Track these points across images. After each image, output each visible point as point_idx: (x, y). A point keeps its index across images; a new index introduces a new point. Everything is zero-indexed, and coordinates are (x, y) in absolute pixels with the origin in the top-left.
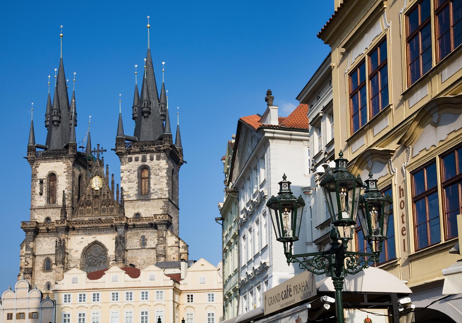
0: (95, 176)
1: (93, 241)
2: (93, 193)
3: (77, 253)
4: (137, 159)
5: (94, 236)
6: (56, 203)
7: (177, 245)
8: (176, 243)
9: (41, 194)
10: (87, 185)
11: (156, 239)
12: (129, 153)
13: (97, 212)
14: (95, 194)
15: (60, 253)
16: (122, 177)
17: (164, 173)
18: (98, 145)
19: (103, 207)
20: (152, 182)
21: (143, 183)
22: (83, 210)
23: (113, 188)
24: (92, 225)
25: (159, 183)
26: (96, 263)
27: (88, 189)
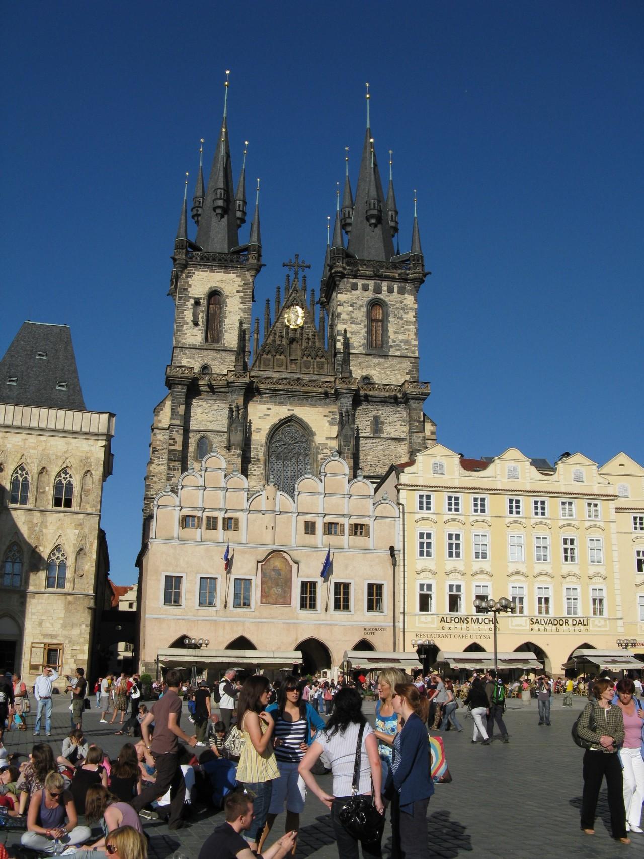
0: (292, 305)
1: (288, 415)
2: (287, 333)
4: (365, 288)
5: (290, 407)
7: (434, 437)
8: (433, 433)
9: (196, 324)
10: (278, 319)
11: (399, 424)
12: (355, 277)
13: (293, 366)
14: (291, 335)
15: (236, 429)
16: (340, 313)
17: (410, 316)
18: (297, 256)
19: (305, 358)
20: (391, 329)
21: (373, 328)
22: (269, 360)
23: (323, 330)
24: (289, 387)
25: (403, 330)
26: (291, 455)
27: (278, 325)
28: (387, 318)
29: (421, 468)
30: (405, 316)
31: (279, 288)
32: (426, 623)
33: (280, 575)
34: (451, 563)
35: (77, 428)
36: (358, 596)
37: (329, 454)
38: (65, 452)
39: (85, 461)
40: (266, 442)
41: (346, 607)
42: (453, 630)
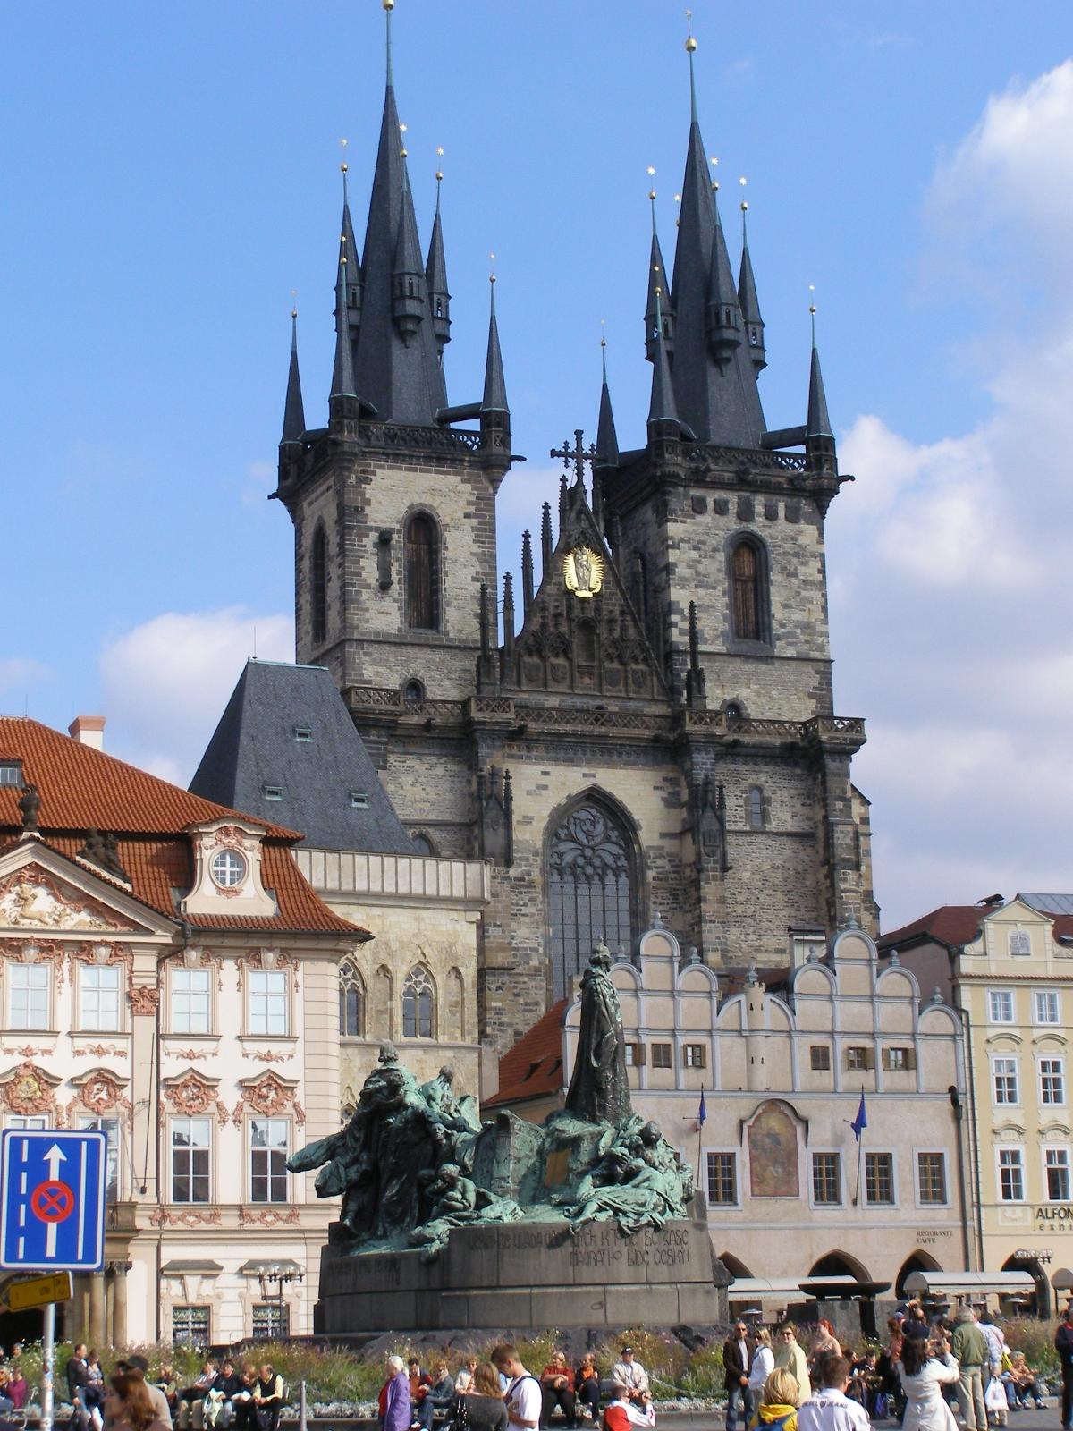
0: (579, 546)
2: (570, 607)
3: (528, 827)
4: (721, 509)
5: (586, 770)
6: (442, 628)
9: (385, 586)
11: (798, 802)
13: (587, 680)
16: (675, 565)
18: (579, 434)
19: (608, 665)
20: (777, 597)
22: (538, 669)
26: (589, 870)
27: (551, 589)
28: (767, 575)
29: (990, 946)
30: (802, 570)
31: (546, 507)
32: (1015, 1220)
33: (779, 1143)
34: (1050, 1113)
35: (431, 891)
36: (906, 1177)
37: (668, 868)
38: (415, 935)
39: (449, 951)
40: (543, 845)
41: (888, 1197)
42: (1057, 1231)
